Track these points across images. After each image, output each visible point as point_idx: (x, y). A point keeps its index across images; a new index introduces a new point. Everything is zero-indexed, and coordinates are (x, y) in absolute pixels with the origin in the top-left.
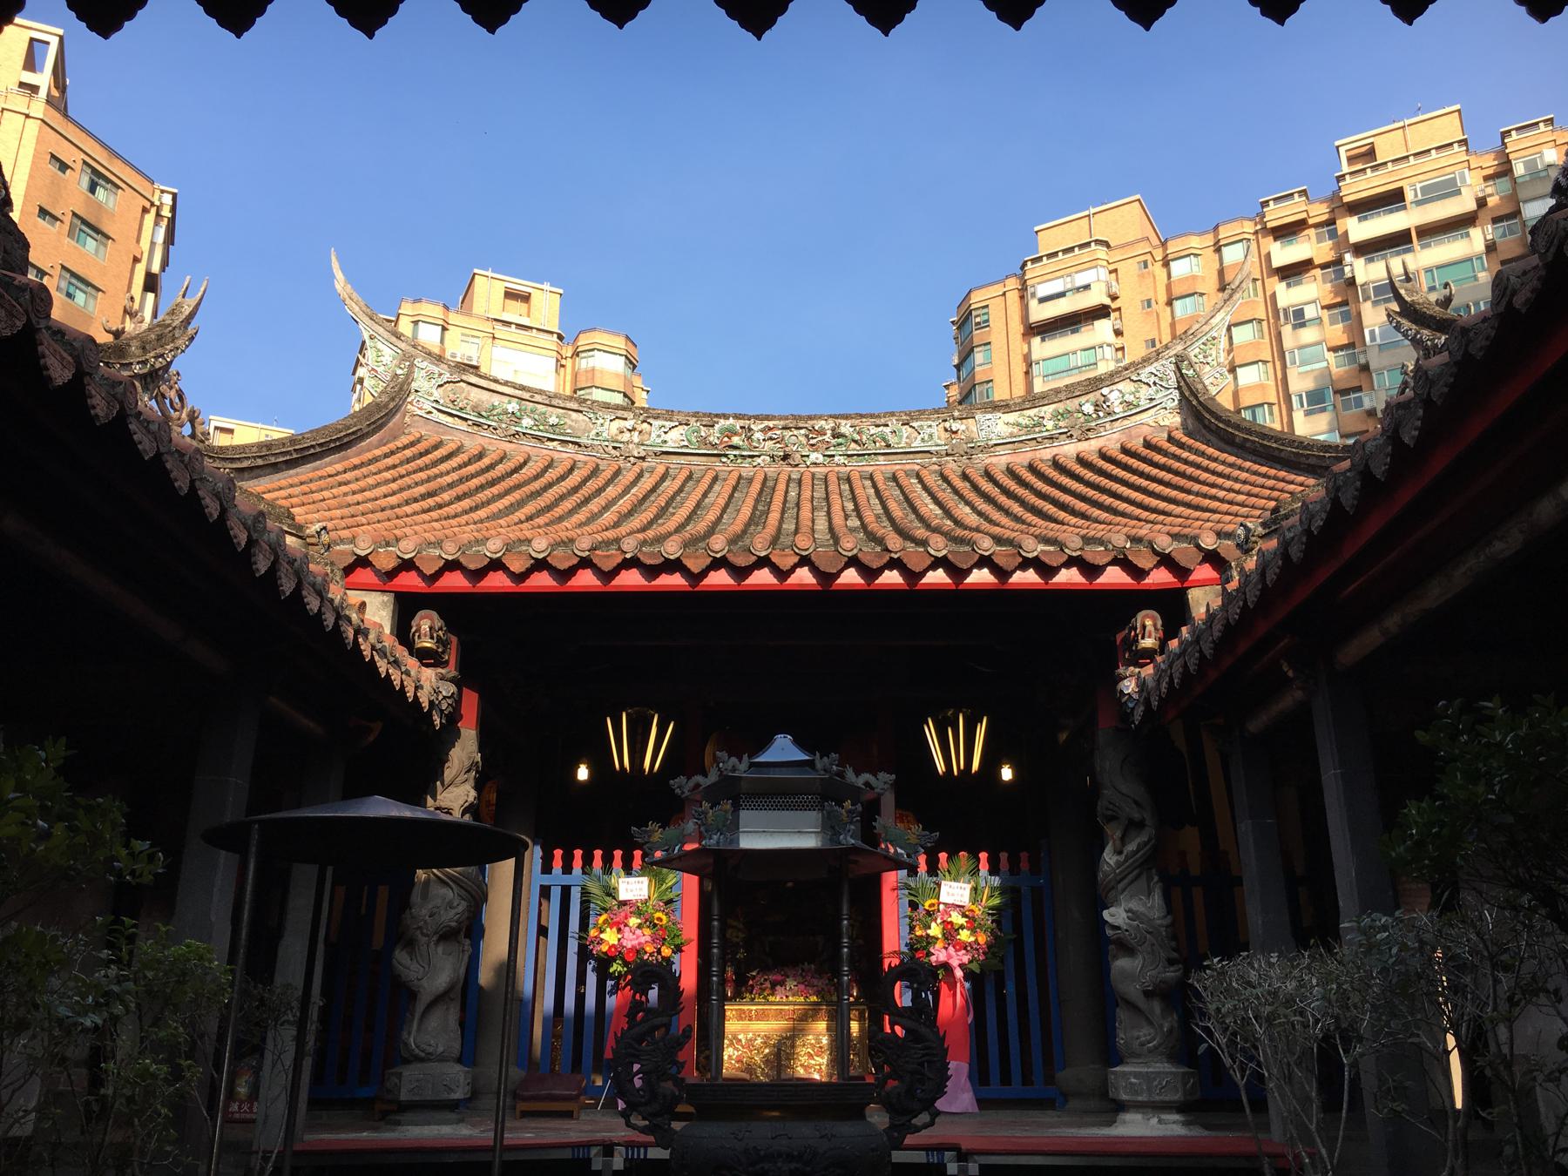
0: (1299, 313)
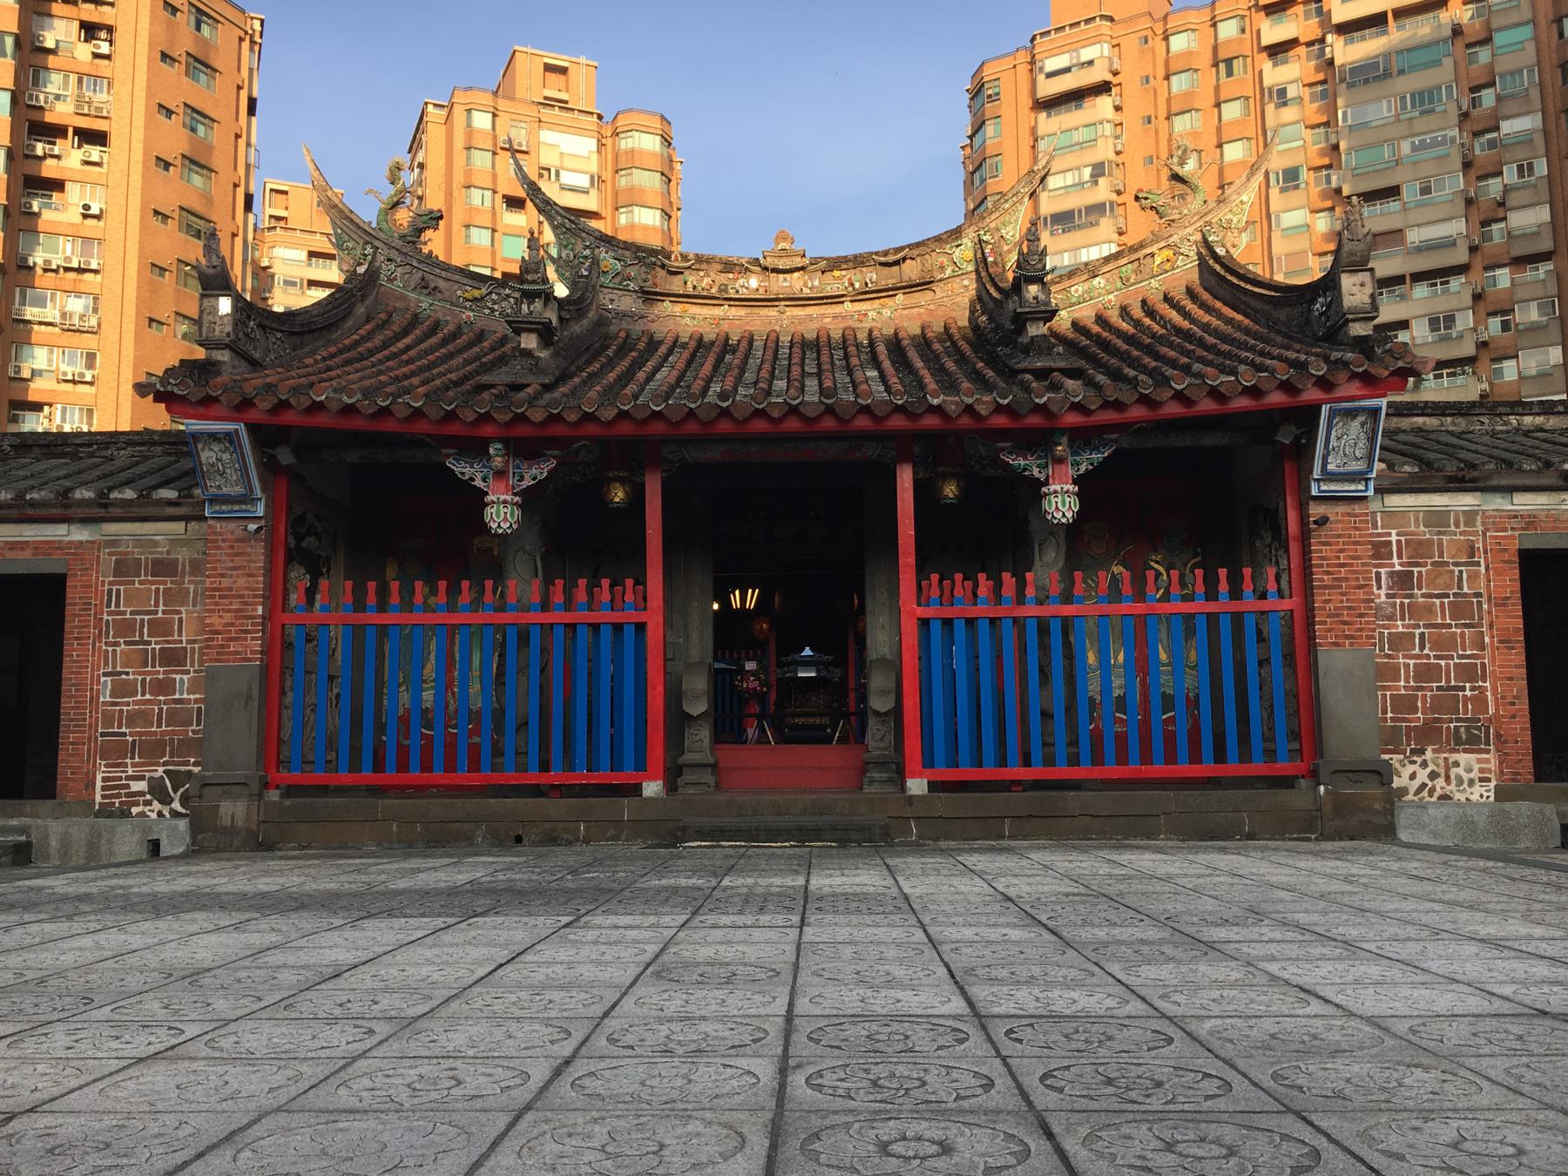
0: (1282, 92)
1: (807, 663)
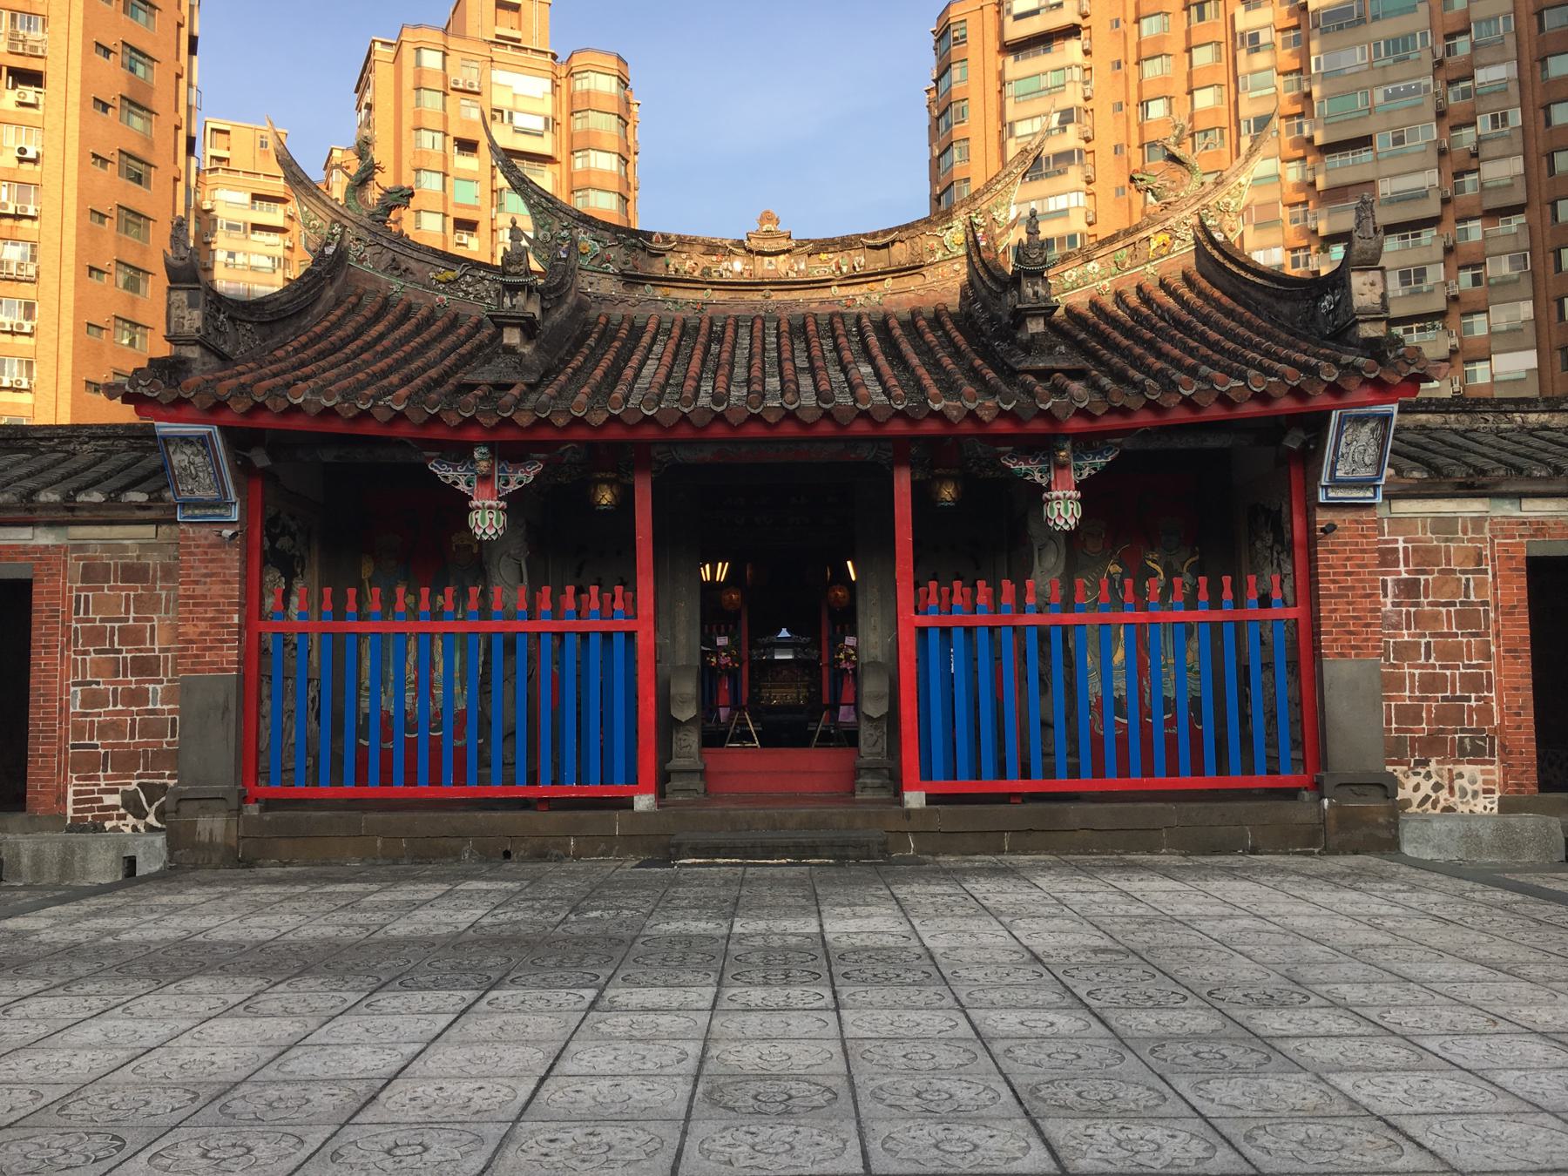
0: (1255, 38)
1: (784, 645)
